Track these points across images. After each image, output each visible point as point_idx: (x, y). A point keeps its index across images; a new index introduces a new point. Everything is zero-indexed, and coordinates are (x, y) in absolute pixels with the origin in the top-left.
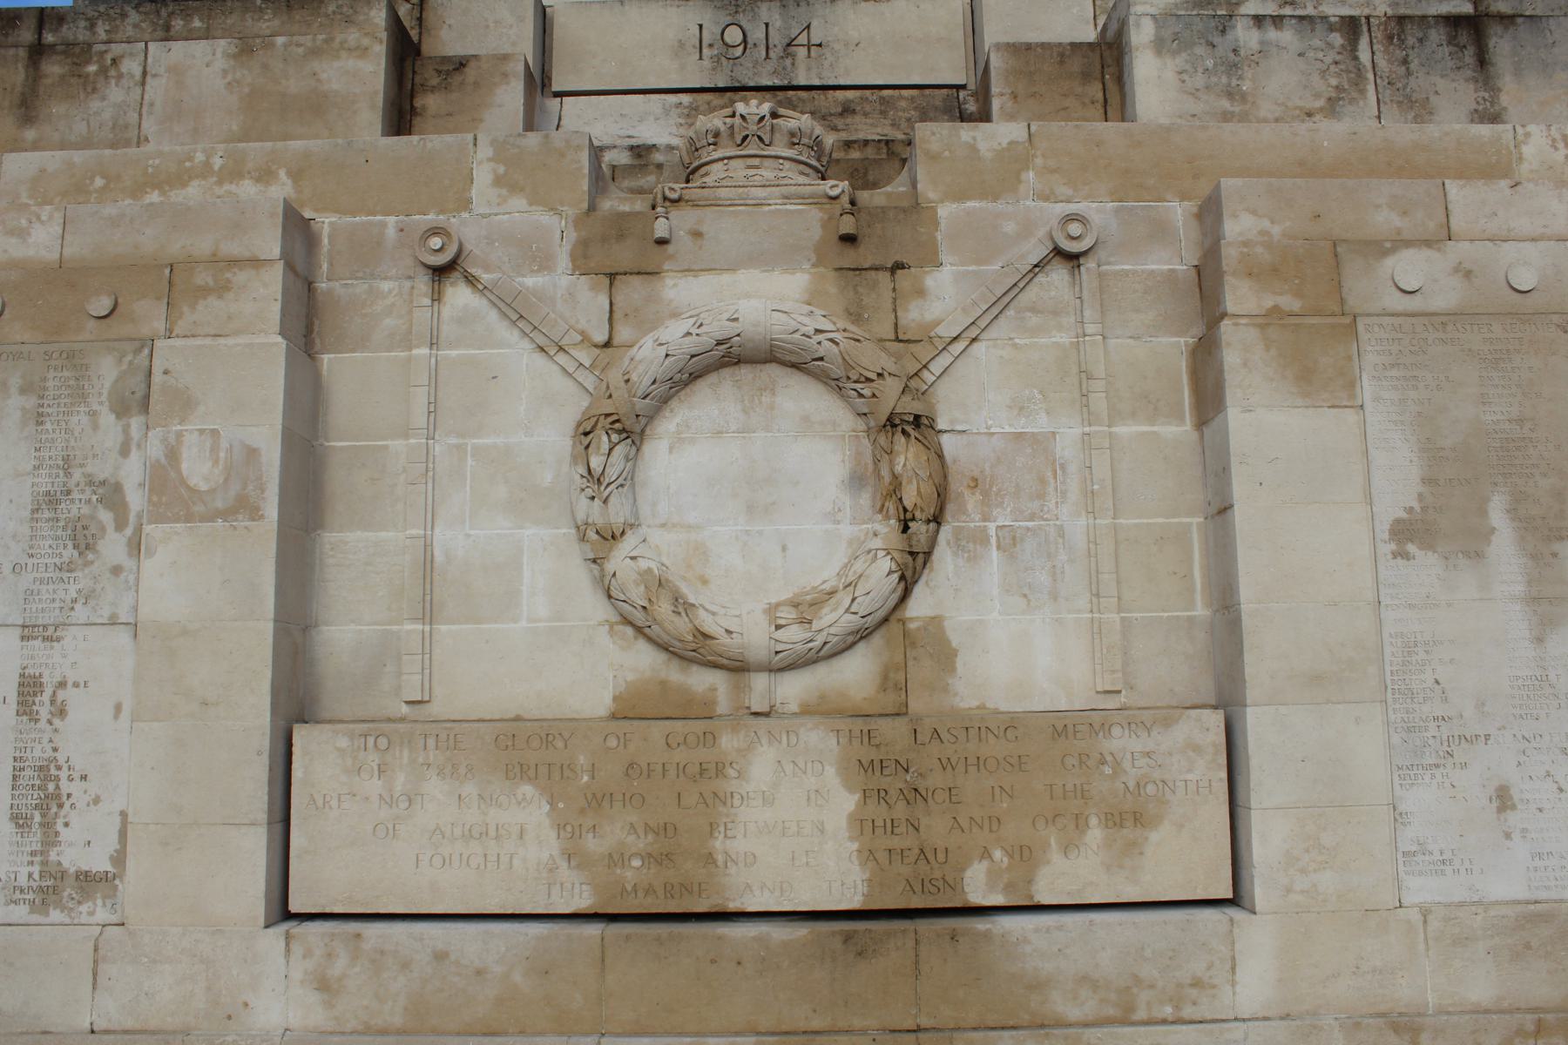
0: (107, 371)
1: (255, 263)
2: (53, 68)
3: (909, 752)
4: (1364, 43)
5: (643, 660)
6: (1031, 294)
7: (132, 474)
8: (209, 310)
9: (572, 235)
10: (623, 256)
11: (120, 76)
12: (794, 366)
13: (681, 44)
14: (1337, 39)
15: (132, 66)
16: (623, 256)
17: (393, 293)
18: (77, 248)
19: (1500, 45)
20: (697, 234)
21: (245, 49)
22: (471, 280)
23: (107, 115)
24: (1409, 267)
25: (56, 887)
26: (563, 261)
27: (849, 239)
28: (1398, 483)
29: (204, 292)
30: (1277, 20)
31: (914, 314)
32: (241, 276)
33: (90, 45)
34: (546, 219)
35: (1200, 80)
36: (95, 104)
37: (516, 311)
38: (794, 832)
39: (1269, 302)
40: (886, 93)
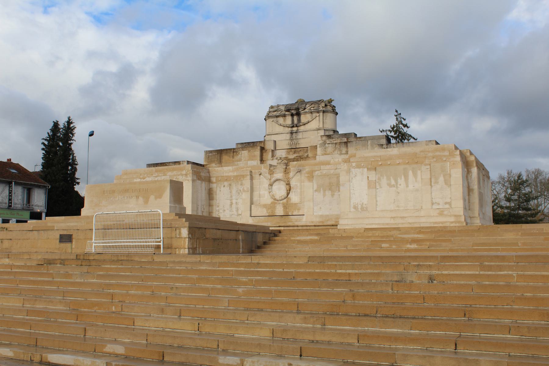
0: (240, 183)
2: (235, 154)
5: (273, 200)
7: (242, 189)
19: (349, 144)
21: (249, 151)
24: (317, 173)
25: (238, 215)
28: (315, 187)
37: (265, 177)
38: (280, 211)
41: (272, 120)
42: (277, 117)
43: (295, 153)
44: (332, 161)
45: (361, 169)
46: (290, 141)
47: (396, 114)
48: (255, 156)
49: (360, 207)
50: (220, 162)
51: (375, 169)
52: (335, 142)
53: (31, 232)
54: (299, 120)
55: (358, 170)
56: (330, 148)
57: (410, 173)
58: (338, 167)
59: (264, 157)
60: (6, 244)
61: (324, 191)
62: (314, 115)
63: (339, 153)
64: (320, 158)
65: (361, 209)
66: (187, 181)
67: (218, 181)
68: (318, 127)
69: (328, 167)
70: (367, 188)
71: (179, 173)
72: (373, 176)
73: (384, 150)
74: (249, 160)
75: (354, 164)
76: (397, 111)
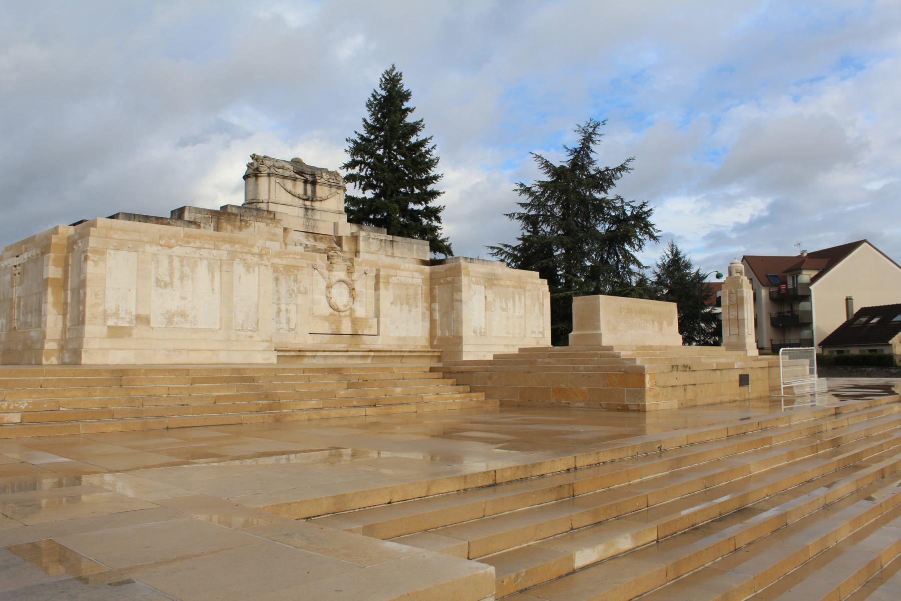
3: (355, 321)
24: (394, 278)
25: (290, 330)
28: (391, 299)
37: (321, 274)
38: (347, 328)
41: (278, 180)
42: (285, 177)
44: (402, 267)
46: (304, 220)
54: (314, 192)
57: (517, 297)
60: (690, 393)
61: (402, 304)
62: (334, 190)
66: (263, 267)
71: (246, 250)
75: (474, 279)
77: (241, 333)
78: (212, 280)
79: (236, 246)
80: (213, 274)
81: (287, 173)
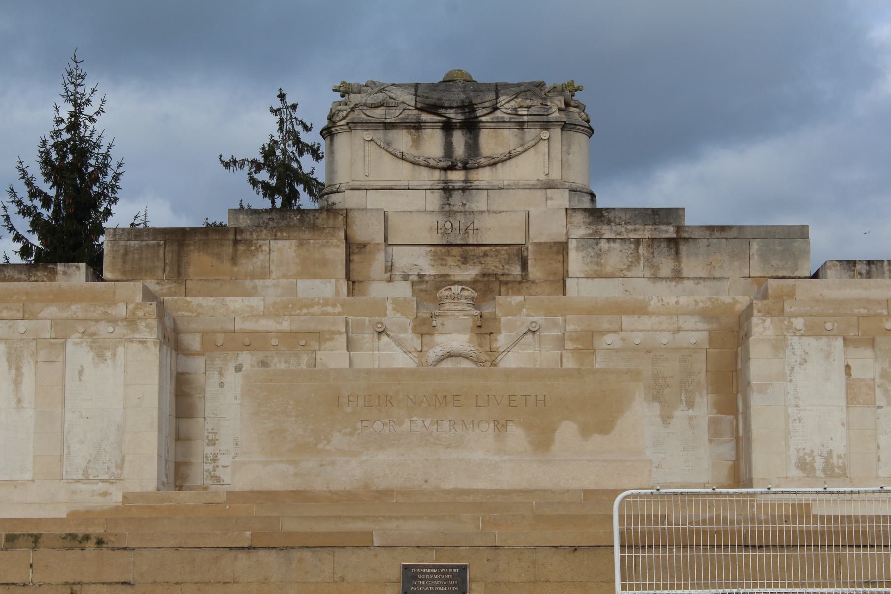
1: (340, 333)
2: (241, 248)
4: (641, 247)
6: (523, 340)
8: (329, 344)
9: (412, 324)
10: (425, 329)
11: (262, 251)
12: (466, 358)
13: (431, 228)
14: (632, 246)
15: (265, 248)
16: (425, 329)
17: (368, 337)
18: (294, 327)
19: (683, 248)
20: (443, 324)
21: (301, 243)
22: (388, 335)
23: (259, 264)
24: (609, 338)
26: (410, 331)
27: (479, 327)
29: (327, 340)
30: (614, 240)
31: (494, 345)
32: (336, 336)
33: (252, 240)
34: (406, 319)
35: (589, 260)
36: (255, 260)
37: (399, 343)
39: (575, 346)
40: (498, 248)
41: (369, 135)
42: (388, 126)
43: (465, 260)
44: (654, 304)
45: (824, 340)
46: (441, 219)
47: (278, 104)
48: (324, 263)
49: (819, 463)
50: (179, 274)
51: (872, 343)
52: (632, 236)
53: (241, 555)
54: (473, 147)
55: (812, 343)
56: (615, 256)
58: (685, 326)
59: (353, 266)
62: (531, 133)
63: (648, 273)
64: (581, 288)
65: (824, 470)
66: (136, 346)
67: (211, 346)
68: (543, 177)
69: (647, 322)
70: (843, 403)
72: (866, 365)
73: (859, 280)
74: (301, 275)
75: (799, 323)
76: (282, 96)
77: (80, 486)
78: (17, 382)
79: (74, 307)
80: (18, 369)
81: (393, 115)
